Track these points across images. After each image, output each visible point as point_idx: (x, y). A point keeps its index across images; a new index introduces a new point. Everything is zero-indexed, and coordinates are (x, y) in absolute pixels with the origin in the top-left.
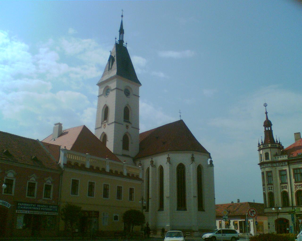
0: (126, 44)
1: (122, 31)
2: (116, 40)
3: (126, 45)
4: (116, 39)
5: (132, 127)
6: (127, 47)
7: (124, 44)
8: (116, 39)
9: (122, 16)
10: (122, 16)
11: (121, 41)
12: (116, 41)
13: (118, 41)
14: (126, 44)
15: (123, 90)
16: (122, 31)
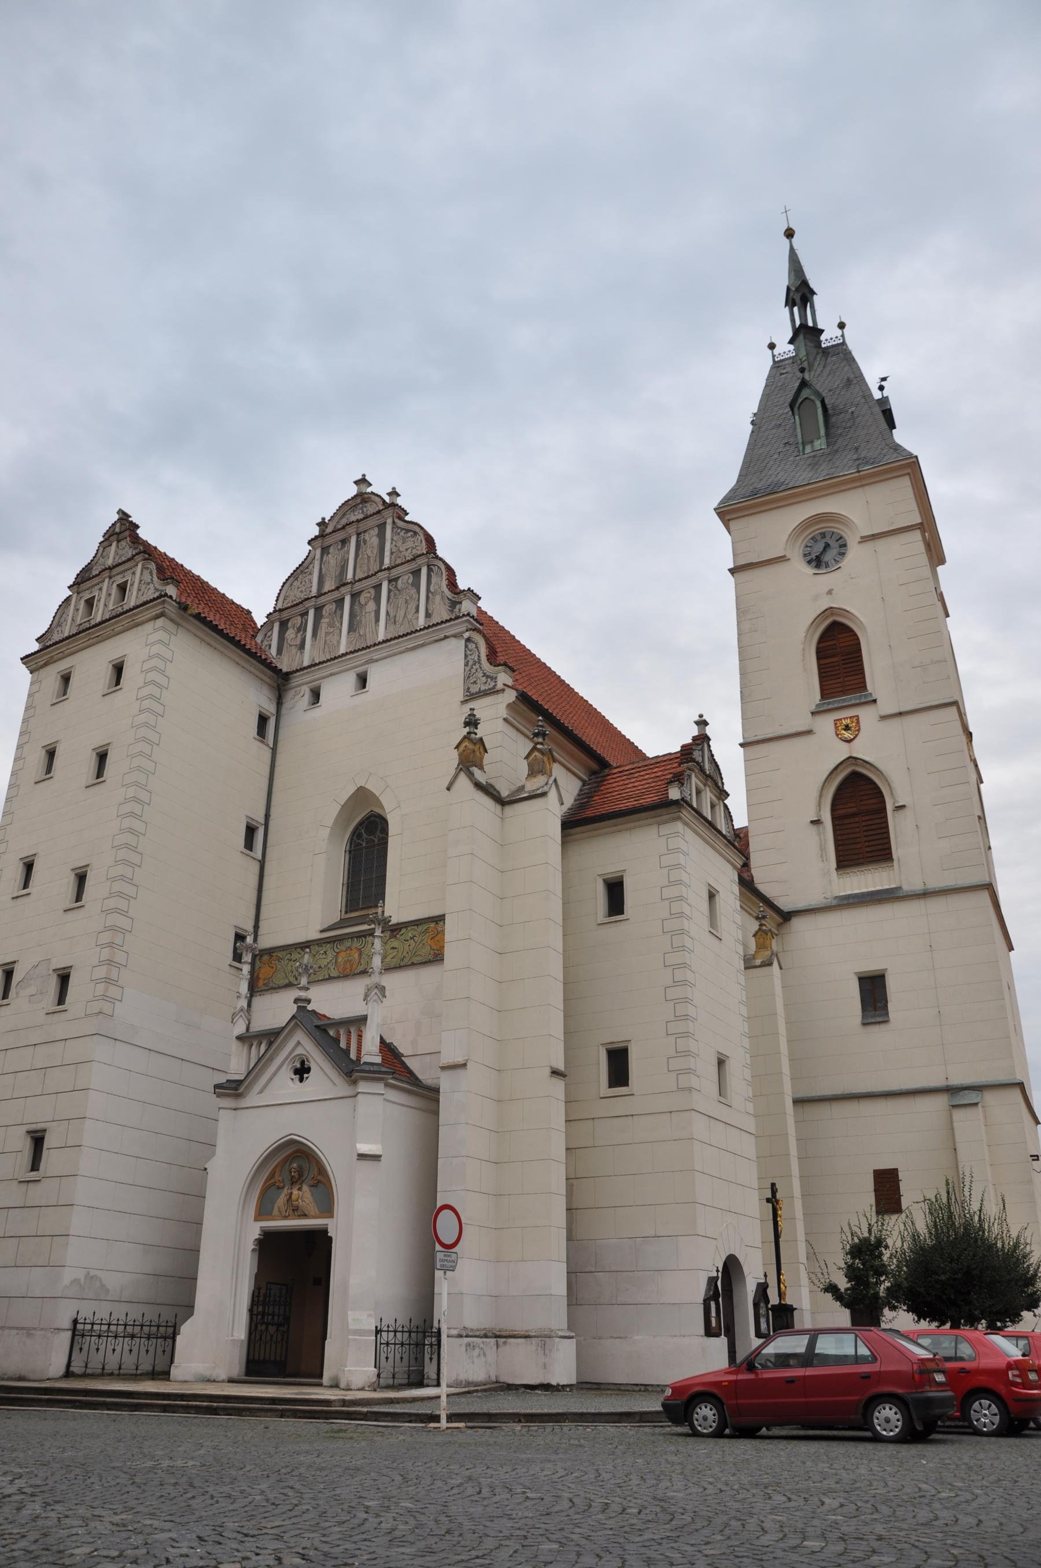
0: (842, 326)
1: (800, 295)
2: (776, 351)
3: (839, 332)
4: (772, 346)
5: (883, 718)
6: (847, 341)
7: (829, 336)
8: (772, 346)
9: (789, 234)
10: (789, 234)
11: (806, 333)
12: (774, 356)
13: (791, 347)
14: (842, 326)
15: (782, 559)
16: (800, 295)
